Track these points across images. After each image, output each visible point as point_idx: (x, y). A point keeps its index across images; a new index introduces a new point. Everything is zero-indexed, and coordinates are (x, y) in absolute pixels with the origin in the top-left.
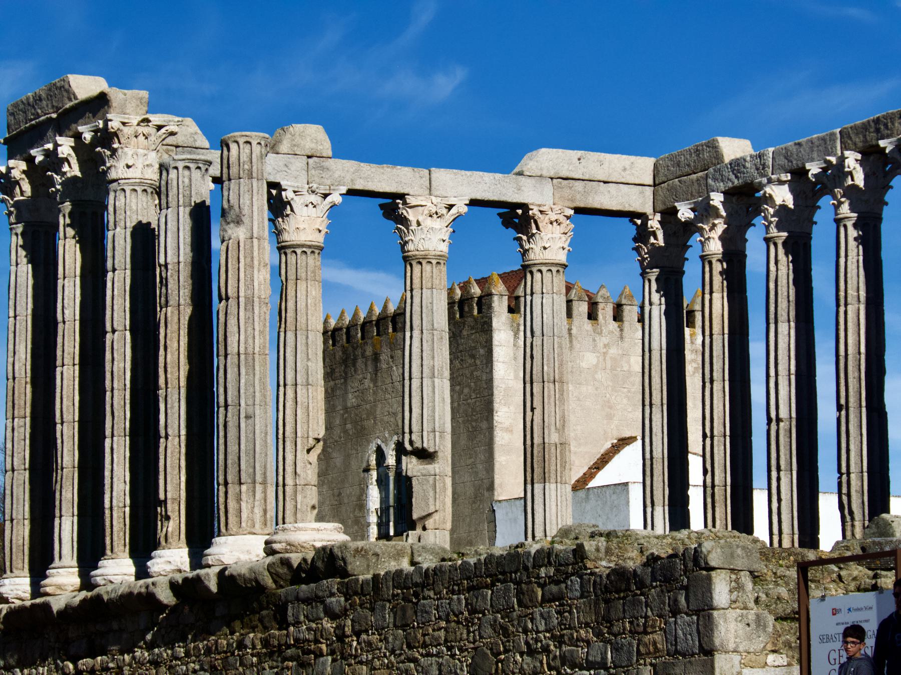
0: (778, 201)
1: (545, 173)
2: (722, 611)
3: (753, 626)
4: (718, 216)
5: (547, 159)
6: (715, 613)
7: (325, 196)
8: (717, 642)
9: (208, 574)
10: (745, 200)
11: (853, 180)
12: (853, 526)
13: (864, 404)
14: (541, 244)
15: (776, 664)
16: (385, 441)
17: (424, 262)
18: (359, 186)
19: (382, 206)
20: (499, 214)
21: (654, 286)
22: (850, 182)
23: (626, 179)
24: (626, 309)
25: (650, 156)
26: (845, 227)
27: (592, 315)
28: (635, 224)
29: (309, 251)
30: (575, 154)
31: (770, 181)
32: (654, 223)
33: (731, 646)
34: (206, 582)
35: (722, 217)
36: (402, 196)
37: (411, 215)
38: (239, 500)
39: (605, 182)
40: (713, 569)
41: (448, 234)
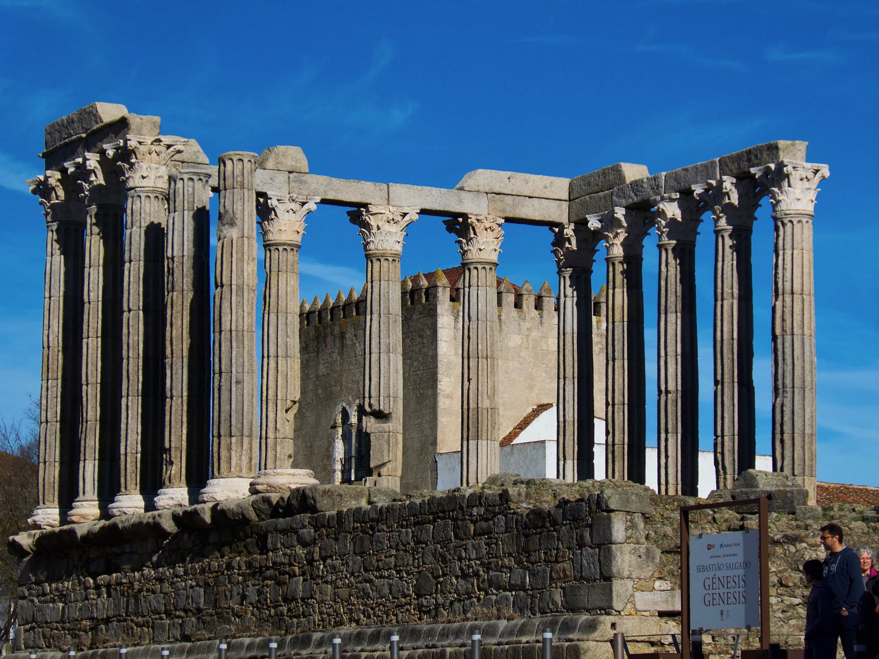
0: (669, 215)
1: (481, 189)
3: (644, 557)
4: (621, 226)
5: (484, 178)
6: (614, 547)
7: (303, 204)
8: (615, 570)
9: (203, 508)
10: (643, 213)
11: (729, 199)
12: (725, 478)
13: (736, 380)
14: (477, 246)
15: (662, 588)
16: (349, 404)
17: (382, 259)
18: (330, 196)
19: (349, 213)
20: (444, 222)
21: (568, 282)
22: (727, 201)
23: (546, 195)
24: (546, 300)
26: (723, 237)
27: (518, 305)
28: (554, 231)
29: (289, 249)
31: (663, 199)
32: (569, 231)
33: (626, 574)
34: (202, 515)
35: (623, 227)
36: (365, 205)
37: (373, 221)
38: (230, 449)
39: (530, 197)
40: (613, 511)
41: (402, 237)
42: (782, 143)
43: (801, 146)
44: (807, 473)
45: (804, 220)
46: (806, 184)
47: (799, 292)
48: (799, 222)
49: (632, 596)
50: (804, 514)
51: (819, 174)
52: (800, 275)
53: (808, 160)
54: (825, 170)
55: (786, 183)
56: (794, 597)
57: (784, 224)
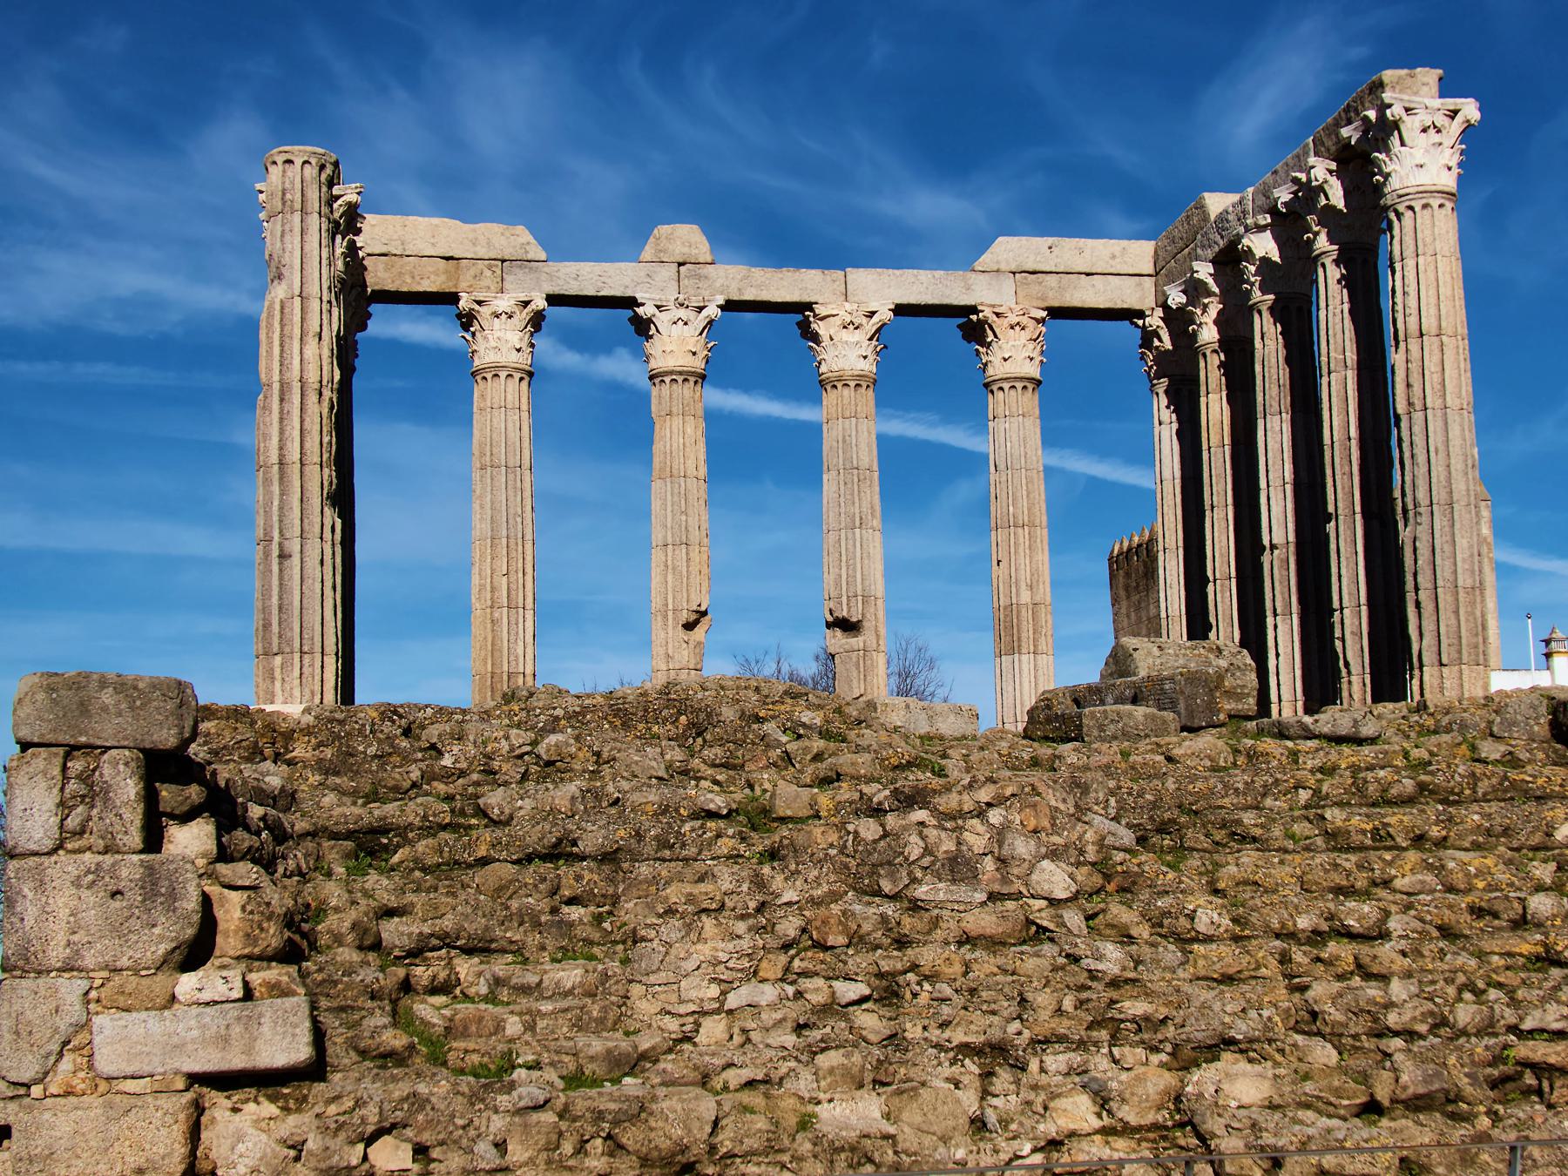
0: (1259, 253)
1: (1003, 267)
2: (32, 861)
4: (1210, 294)
5: (1009, 250)
7: (701, 309)
10: (1230, 259)
11: (1327, 198)
12: (1350, 682)
13: (1358, 509)
14: (1000, 355)
15: (206, 996)
17: (839, 385)
21: (1164, 401)
22: (1323, 202)
23: (1115, 267)
25: (1150, 239)
26: (1323, 265)
28: (1137, 326)
29: (680, 379)
30: (1043, 242)
31: (1247, 229)
32: (1155, 320)
33: (56, 954)
35: (1214, 294)
36: (809, 306)
37: (820, 328)
41: (871, 348)
42: (1388, 75)
43: (1429, 77)
44: (1465, 658)
45: (1435, 203)
46: (1433, 136)
47: (1434, 332)
48: (1425, 206)
49: (84, 1026)
50: (1101, 728)
51: (1459, 118)
52: (1433, 300)
53: (1443, 94)
54: (1470, 110)
55: (1395, 140)
56: (847, 978)
57: (1399, 215)
